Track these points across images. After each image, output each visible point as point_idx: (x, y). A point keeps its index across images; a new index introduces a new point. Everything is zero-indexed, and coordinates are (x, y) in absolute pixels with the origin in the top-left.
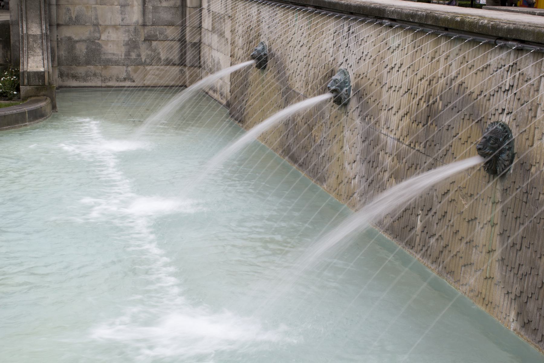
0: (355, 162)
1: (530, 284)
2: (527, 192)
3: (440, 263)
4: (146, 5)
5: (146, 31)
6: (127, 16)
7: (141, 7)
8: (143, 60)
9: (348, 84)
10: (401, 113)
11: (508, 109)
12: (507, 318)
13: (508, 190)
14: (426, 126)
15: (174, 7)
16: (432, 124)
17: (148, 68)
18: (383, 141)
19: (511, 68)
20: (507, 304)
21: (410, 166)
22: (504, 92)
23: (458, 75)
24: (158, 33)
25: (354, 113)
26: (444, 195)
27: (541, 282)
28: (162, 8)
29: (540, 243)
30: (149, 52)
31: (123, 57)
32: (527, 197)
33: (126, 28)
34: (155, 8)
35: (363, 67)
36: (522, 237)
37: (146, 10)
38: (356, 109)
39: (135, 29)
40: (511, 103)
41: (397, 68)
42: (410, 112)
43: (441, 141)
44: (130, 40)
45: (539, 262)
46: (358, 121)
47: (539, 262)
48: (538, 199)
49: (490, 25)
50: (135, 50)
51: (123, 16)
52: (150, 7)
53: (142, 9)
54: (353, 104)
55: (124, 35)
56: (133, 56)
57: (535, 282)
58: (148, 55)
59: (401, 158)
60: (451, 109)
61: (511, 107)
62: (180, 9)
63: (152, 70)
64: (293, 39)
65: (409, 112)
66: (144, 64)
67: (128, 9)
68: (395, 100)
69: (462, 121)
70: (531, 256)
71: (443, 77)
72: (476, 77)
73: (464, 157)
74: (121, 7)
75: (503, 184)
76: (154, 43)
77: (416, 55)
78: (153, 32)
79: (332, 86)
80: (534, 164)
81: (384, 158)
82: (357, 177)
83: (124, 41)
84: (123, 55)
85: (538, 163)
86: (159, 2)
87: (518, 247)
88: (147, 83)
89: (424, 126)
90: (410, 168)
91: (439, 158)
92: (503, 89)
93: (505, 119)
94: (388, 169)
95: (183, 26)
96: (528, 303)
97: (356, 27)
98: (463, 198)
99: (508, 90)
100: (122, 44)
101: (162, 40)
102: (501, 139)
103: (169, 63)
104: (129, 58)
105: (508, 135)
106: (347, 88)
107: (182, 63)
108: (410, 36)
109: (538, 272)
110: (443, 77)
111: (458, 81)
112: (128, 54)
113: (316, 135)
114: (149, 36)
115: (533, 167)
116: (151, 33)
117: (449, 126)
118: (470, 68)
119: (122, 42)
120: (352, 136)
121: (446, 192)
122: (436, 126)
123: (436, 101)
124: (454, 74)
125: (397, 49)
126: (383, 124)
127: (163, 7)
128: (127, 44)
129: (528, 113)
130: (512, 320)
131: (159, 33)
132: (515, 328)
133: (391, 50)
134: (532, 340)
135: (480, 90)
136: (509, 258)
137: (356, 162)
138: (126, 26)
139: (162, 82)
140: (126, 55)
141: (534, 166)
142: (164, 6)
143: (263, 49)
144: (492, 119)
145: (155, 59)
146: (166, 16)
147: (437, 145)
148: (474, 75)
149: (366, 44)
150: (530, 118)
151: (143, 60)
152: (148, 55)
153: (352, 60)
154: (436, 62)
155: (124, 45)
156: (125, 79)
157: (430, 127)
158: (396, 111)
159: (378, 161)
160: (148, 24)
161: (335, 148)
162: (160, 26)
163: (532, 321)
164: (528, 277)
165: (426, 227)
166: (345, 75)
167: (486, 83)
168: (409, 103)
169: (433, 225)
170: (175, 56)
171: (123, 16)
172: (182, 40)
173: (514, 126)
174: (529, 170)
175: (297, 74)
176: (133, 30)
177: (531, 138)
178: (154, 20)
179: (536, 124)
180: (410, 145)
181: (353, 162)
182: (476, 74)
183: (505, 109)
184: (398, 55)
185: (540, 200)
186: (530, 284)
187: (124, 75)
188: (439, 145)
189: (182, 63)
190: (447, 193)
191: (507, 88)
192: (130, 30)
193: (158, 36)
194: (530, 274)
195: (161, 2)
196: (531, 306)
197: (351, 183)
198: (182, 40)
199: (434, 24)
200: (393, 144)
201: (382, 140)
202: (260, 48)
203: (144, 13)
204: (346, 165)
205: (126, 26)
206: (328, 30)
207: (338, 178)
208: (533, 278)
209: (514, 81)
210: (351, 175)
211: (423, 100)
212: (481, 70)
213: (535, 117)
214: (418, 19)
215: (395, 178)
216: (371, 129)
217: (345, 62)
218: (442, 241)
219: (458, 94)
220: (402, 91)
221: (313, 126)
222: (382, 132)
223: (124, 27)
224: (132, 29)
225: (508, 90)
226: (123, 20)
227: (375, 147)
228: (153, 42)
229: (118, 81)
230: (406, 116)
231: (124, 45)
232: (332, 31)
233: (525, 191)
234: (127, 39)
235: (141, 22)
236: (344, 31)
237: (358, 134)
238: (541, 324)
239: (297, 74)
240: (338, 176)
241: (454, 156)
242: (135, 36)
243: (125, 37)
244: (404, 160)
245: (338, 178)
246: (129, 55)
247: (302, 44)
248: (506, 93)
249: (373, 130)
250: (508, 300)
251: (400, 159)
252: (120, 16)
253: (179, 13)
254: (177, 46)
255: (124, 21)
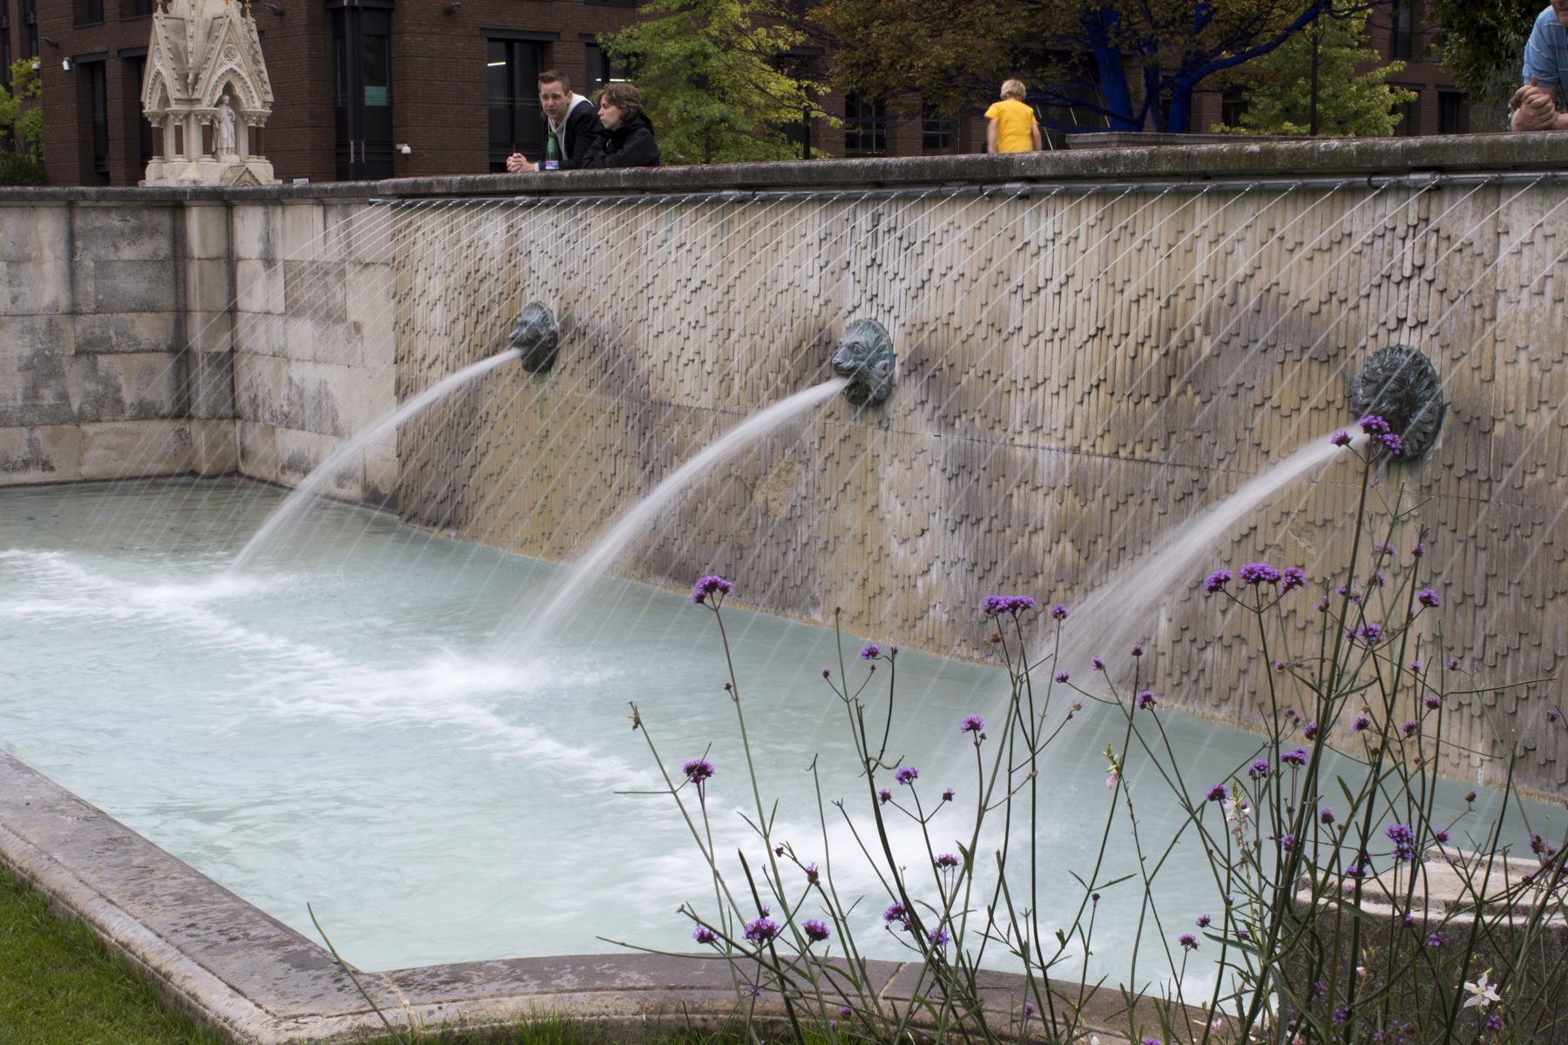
0: (923, 531)
1: (1521, 671)
2: (1489, 479)
3: (1242, 700)
4: (77, 259)
5: (79, 329)
6: (25, 289)
7: (62, 264)
8: (75, 408)
9: (886, 352)
10: (1078, 387)
11: (1416, 315)
12: (1464, 763)
13: (1435, 487)
14: (1164, 403)
15: (154, 261)
16: (1182, 392)
17: (89, 429)
18: (1023, 464)
19: (1411, 231)
20: (1460, 732)
21: (1122, 500)
22: (1398, 284)
23: (1257, 272)
24: (112, 333)
25: (909, 418)
26: (1239, 542)
27: (1552, 657)
28: (120, 265)
29: (1539, 577)
30: (91, 386)
31: (19, 402)
32: (1490, 489)
33: (26, 324)
34: (102, 265)
35: (931, 306)
36: (1487, 575)
37: (78, 272)
38: (919, 407)
39: (50, 323)
40: (1423, 302)
41: (1054, 286)
42: (1110, 380)
43: (1215, 424)
44: (37, 354)
45: (1540, 617)
46: (927, 435)
47: (1540, 617)
48: (1522, 487)
49: (1353, 148)
50: (53, 382)
51: (16, 290)
52: (87, 262)
53: (66, 270)
54: (907, 395)
55: (20, 342)
56: (48, 397)
57: (1533, 661)
58: (87, 395)
59: (1090, 489)
60: (1240, 349)
61: (1424, 311)
62: (170, 266)
63: (102, 434)
64: (657, 281)
65: (1105, 380)
66: (81, 419)
67: (29, 269)
68: (1056, 363)
69: (1277, 369)
70: (1516, 610)
71: (1207, 283)
72: (1311, 267)
73: (1291, 448)
74: (8, 266)
75: (1418, 477)
76: (103, 361)
77: (1116, 248)
78: (98, 331)
79: (846, 359)
80: (1502, 416)
81: (1027, 502)
82: (934, 569)
83: (20, 358)
84: (19, 397)
85: (1512, 412)
86: (113, 249)
87: (1478, 600)
88: (87, 470)
89: (1158, 402)
90: (1121, 507)
91: (1215, 461)
92: (1396, 277)
93: (1408, 339)
94: (1046, 525)
95: (182, 314)
96: (1520, 713)
97: (897, 216)
98: (1299, 536)
99: (1409, 278)
100: (15, 368)
101: (125, 352)
102: (1412, 380)
103: (145, 412)
104: (35, 406)
105: (1426, 368)
106: (887, 361)
107: (182, 411)
108: (1091, 213)
109: (1540, 638)
110: (1207, 283)
111: (1261, 280)
112: (32, 393)
113: (770, 498)
114: (89, 342)
115: (1497, 423)
116: (93, 333)
117: (1239, 386)
118: (1292, 251)
119: (15, 361)
120: (909, 473)
121: (1245, 532)
122: (1196, 394)
123: (1193, 340)
124: (1243, 269)
125: (1050, 244)
126: (1018, 422)
127: (124, 261)
128: (28, 366)
129: (1473, 315)
130: (1478, 763)
131: (116, 333)
132: (1488, 778)
133: (1032, 249)
134: (1542, 789)
135: (1326, 291)
136: (1453, 632)
137: (927, 535)
138: (23, 315)
139: (126, 466)
140: (26, 398)
141: (1501, 420)
142: (126, 258)
143: (545, 318)
144: (1369, 347)
145: (107, 404)
146: (133, 286)
147: (1205, 436)
148: (1306, 264)
149: (939, 251)
150: (1478, 323)
151: (75, 408)
152: (87, 395)
153: (893, 293)
154: (1182, 252)
155: (19, 370)
156: (26, 464)
157: (1176, 401)
158: (1062, 384)
159: (1010, 513)
160: (84, 308)
161: (850, 516)
162: (117, 312)
163: (1534, 749)
164: (1513, 658)
165: (1187, 629)
166: (876, 331)
167: (1343, 273)
168: (1103, 359)
169: (1213, 619)
170: (161, 392)
171: (16, 290)
172: (180, 351)
173: (1437, 349)
174: (1490, 432)
175: (683, 360)
176: (44, 326)
177: (1487, 364)
178: (101, 297)
179: (1498, 332)
180: (1117, 453)
181: (919, 533)
182: (1311, 259)
183: (1405, 319)
184: (1057, 258)
185: (1526, 487)
186: (1521, 671)
187: (23, 452)
188: (1213, 434)
189: (182, 411)
190: (1247, 536)
191: (1407, 273)
192: (37, 326)
193: (114, 340)
194: (1518, 649)
195: (117, 249)
196: (1532, 716)
197: (915, 586)
198: (180, 351)
199: (1178, 169)
200: (1057, 464)
201: (1020, 461)
202: (534, 318)
203: (72, 278)
204: (894, 547)
205: (23, 315)
206: (797, 236)
207: (864, 585)
208: (1528, 654)
209: (1425, 257)
210: (915, 566)
211: (1152, 341)
212: (1325, 247)
213: (1493, 318)
214: (1125, 165)
215: (1073, 541)
216: (976, 443)
217: (869, 304)
218: (1244, 646)
219: (1259, 312)
220: (1077, 338)
221: (757, 479)
222: (1017, 441)
223: (19, 319)
224: (40, 323)
225: (1409, 278)
226: (14, 300)
227: (995, 484)
228: (99, 357)
229: (6, 470)
230: (1094, 391)
231: (19, 370)
232: (813, 236)
233: (1485, 478)
234: (27, 352)
235: (64, 303)
236: (858, 228)
237: (930, 466)
238: (1561, 747)
239: (683, 360)
240: (865, 580)
241: (1264, 448)
242: (51, 341)
243: (23, 346)
244: (1100, 492)
245: (864, 585)
246: (36, 396)
247: (698, 284)
248: (1402, 286)
249: (982, 444)
250: (1461, 723)
251: (1086, 493)
252: (7, 290)
253: (167, 275)
254: (165, 364)
255: (19, 303)
